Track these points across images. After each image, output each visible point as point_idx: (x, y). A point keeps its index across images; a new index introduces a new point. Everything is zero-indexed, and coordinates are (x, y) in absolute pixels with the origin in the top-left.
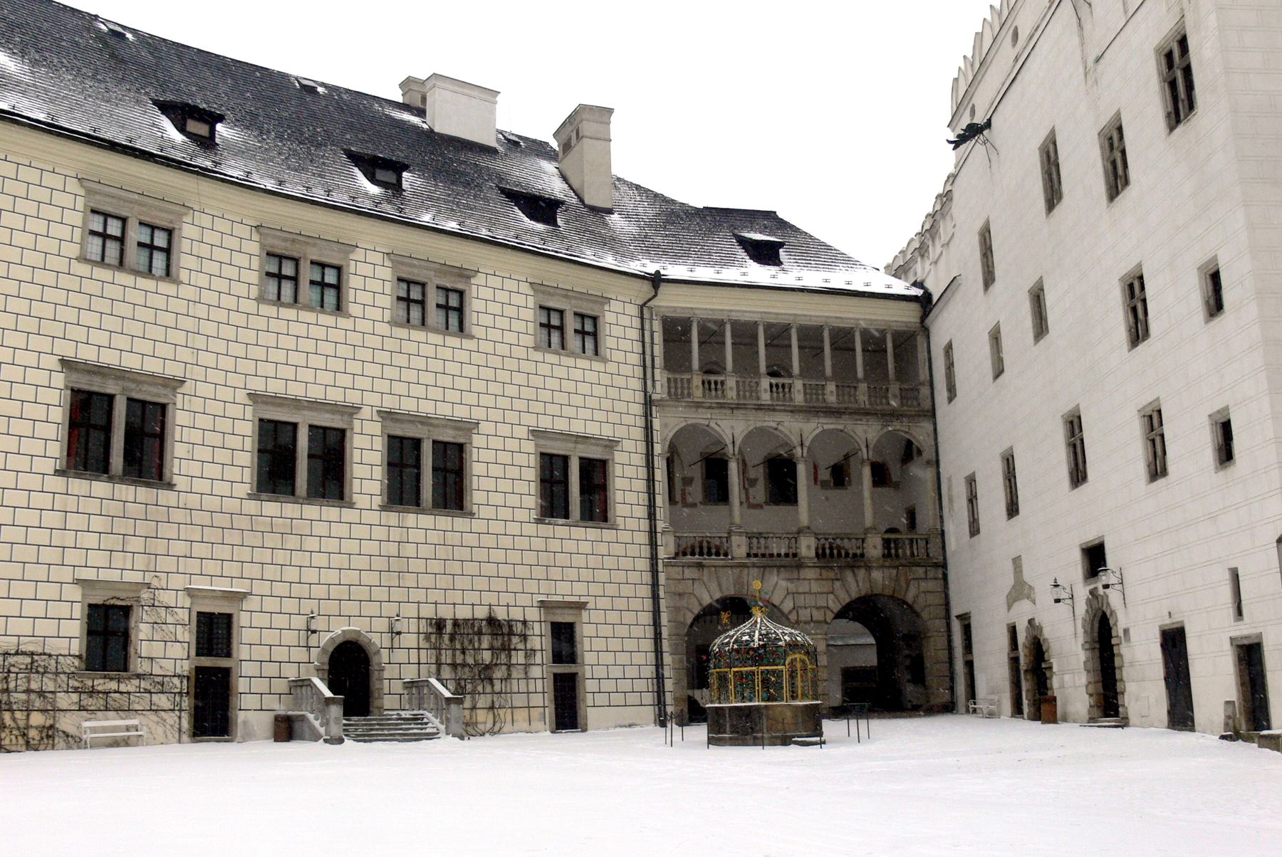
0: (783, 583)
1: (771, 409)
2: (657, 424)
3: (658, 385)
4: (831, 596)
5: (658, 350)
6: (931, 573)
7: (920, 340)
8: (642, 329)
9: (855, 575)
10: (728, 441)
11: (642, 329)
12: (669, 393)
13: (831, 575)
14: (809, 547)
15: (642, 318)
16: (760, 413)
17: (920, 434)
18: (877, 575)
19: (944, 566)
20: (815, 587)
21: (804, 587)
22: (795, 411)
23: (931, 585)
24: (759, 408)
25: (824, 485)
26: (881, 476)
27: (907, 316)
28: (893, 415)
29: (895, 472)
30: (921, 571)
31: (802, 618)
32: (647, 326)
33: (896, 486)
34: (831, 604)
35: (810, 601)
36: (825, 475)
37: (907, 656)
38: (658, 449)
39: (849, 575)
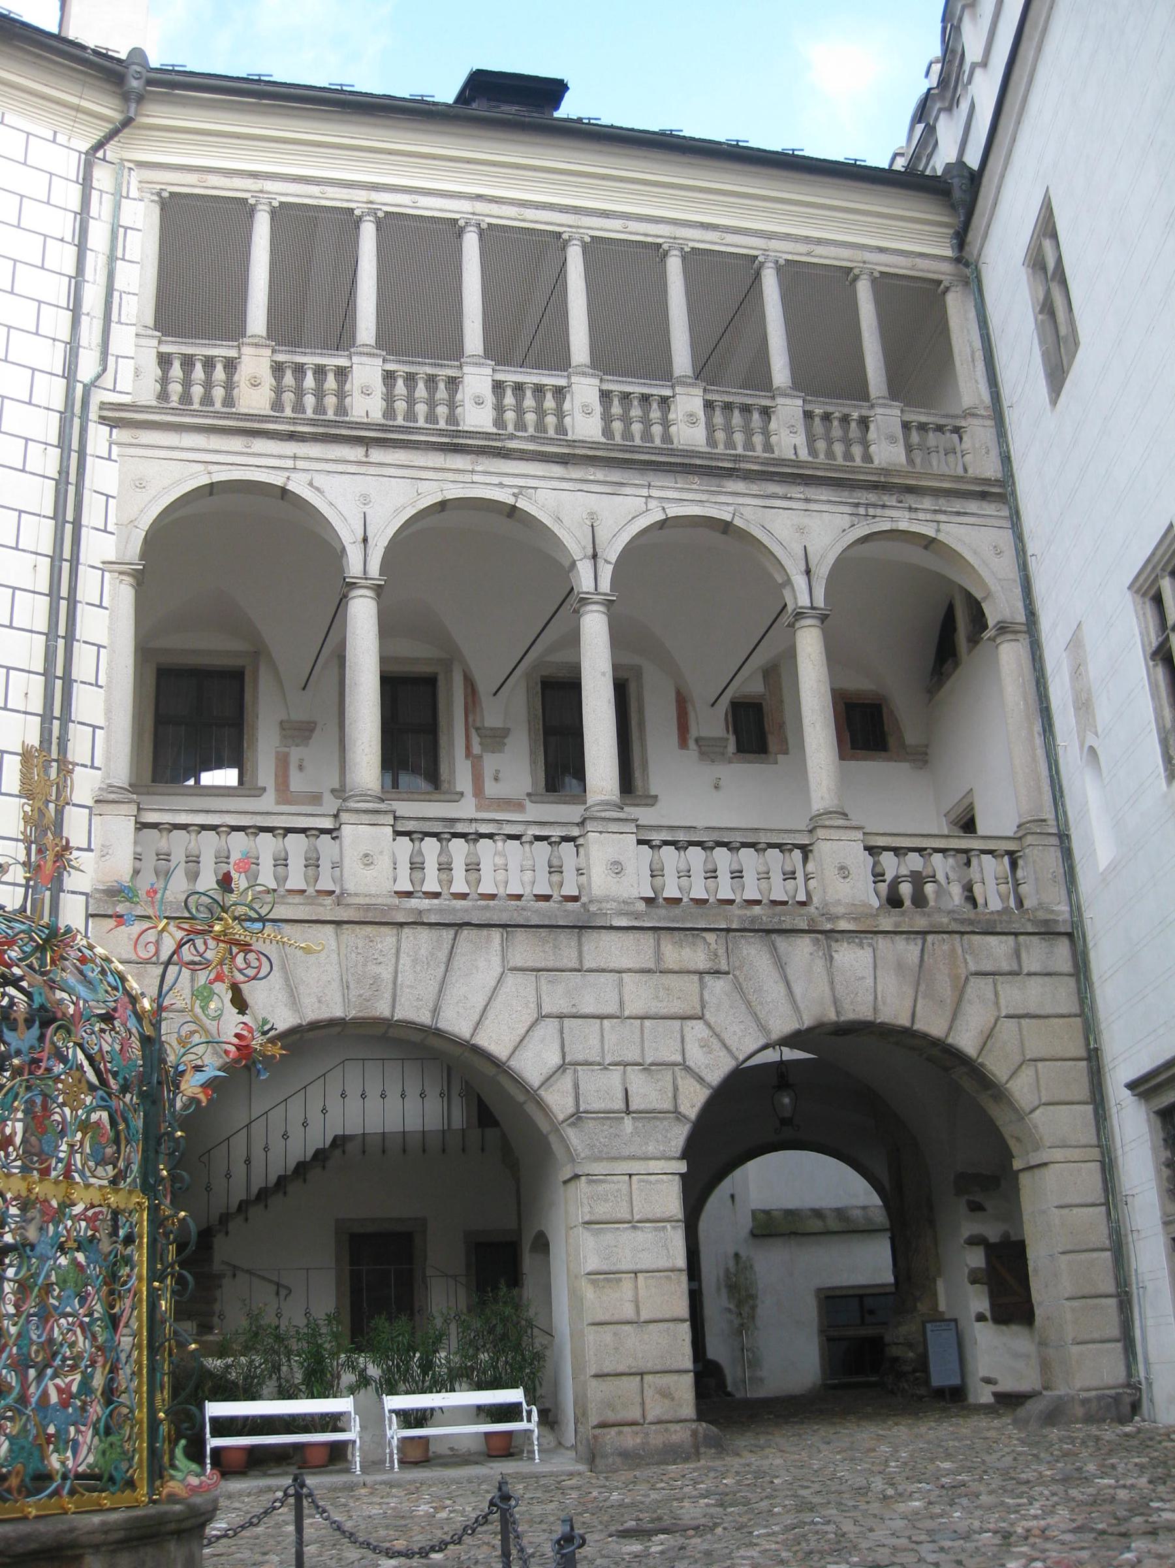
0: (519, 989)
1: (490, 449)
2: (102, 475)
3: (126, 370)
4: (696, 1030)
5: (138, 279)
6: (1036, 955)
7: (958, 308)
8: (83, 214)
9: (780, 965)
10: (348, 534)
11: (83, 214)
12: (163, 395)
13: (696, 956)
14: (617, 868)
15: (86, 184)
16: (459, 461)
17: (973, 539)
18: (852, 959)
19: (1073, 935)
20: (640, 996)
21: (596, 996)
22: (574, 458)
23: (1031, 995)
24: (456, 444)
25: (708, 751)
26: (865, 728)
27: (906, 239)
28: (884, 485)
29: (904, 706)
30: (998, 949)
31: (593, 1101)
32: (101, 207)
33: (921, 757)
34: (696, 1056)
35: (620, 1041)
36: (712, 723)
37: (974, 1241)
38: (98, 547)
39: (754, 953)
